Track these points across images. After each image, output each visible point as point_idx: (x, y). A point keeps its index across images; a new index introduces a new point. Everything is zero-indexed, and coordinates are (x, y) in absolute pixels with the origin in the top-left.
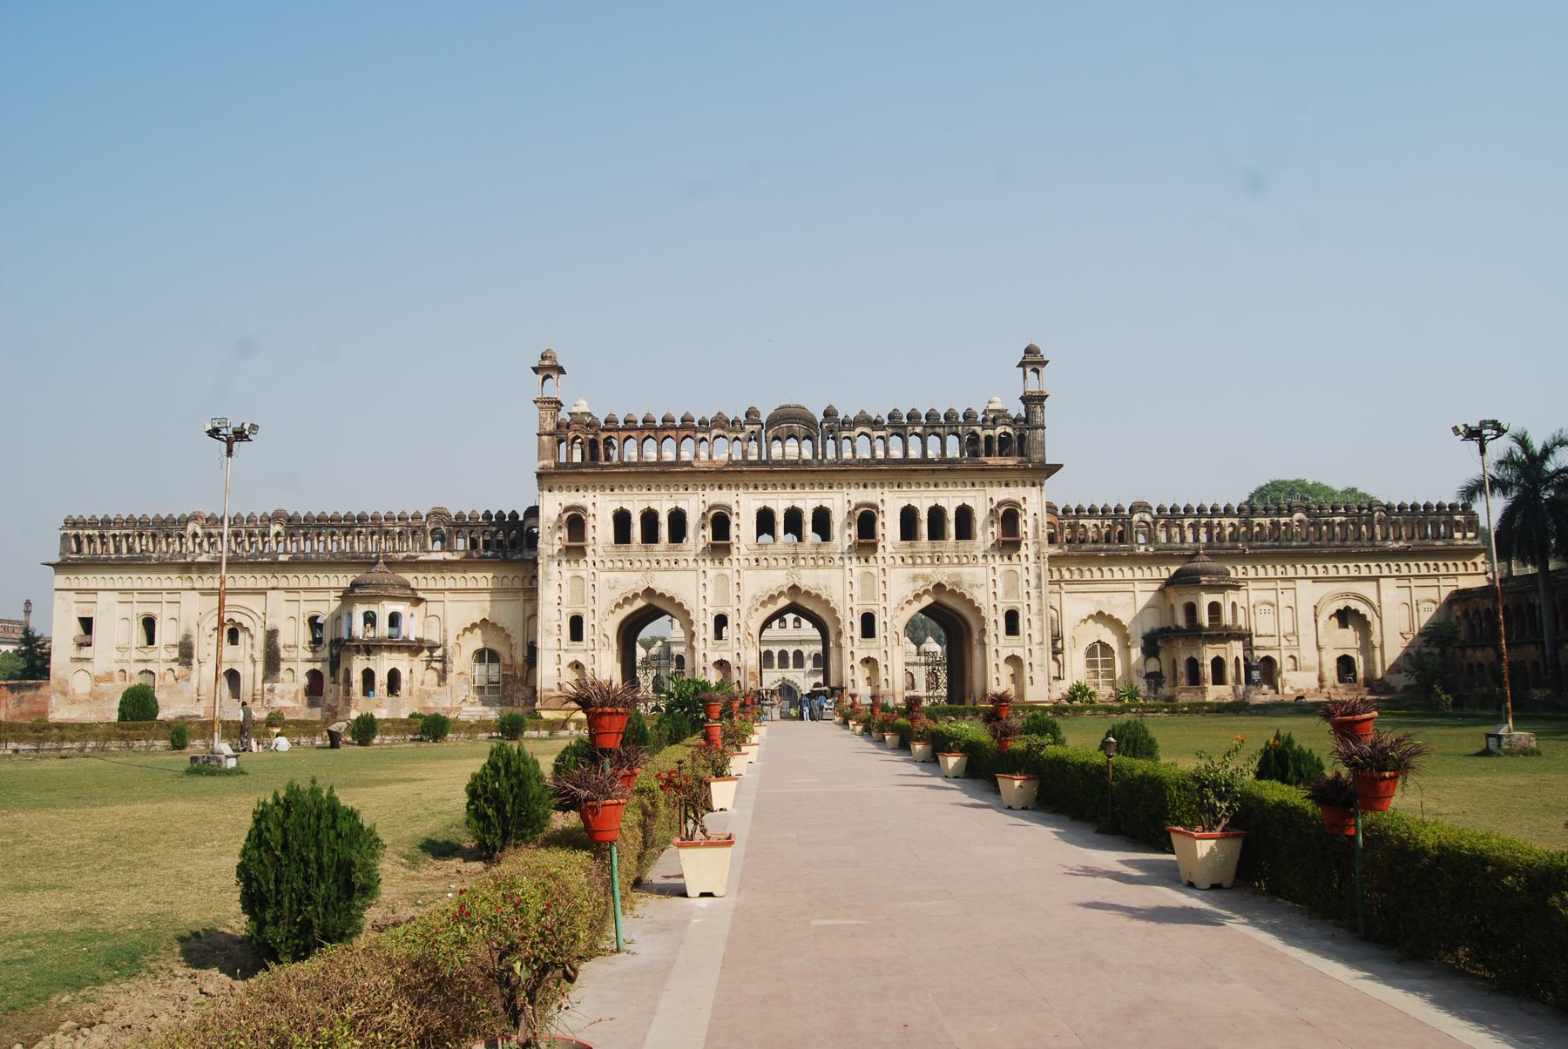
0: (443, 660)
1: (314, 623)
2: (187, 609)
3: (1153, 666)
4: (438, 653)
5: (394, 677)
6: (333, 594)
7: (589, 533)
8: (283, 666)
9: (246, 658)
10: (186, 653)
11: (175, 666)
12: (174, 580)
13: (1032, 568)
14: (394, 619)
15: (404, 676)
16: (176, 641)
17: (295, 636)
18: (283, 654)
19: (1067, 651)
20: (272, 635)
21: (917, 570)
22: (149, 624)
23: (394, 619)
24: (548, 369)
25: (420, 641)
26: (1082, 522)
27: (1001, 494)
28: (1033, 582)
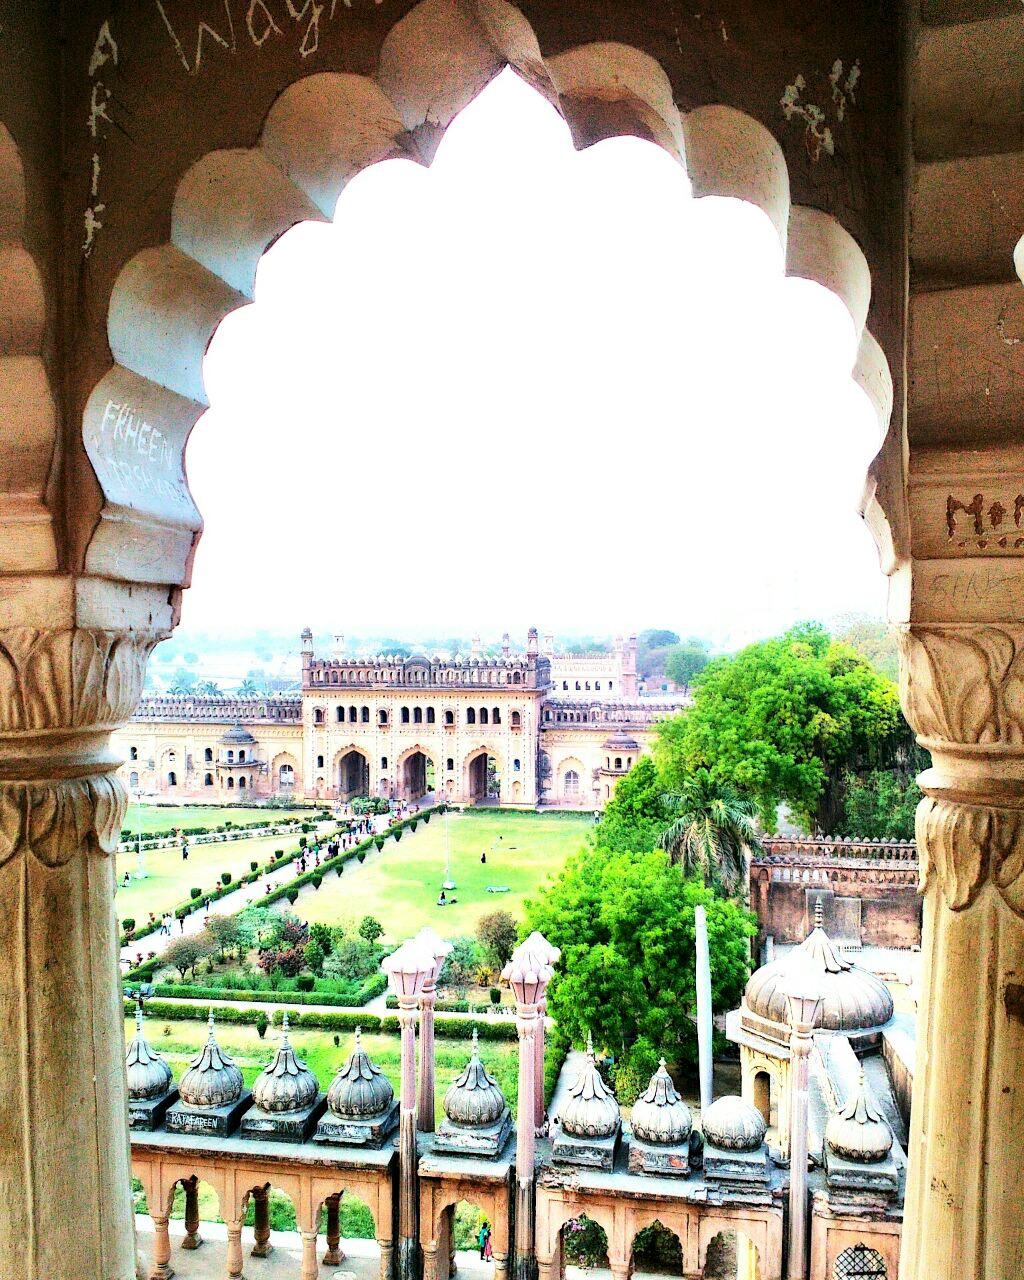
0: (267, 770)
1: (209, 752)
3: (597, 785)
4: (264, 767)
5: (242, 780)
6: (215, 739)
7: (326, 717)
8: (195, 771)
10: (152, 764)
13: (527, 741)
14: (242, 754)
15: (248, 779)
18: (195, 766)
19: (554, 778)
20: (189, 757)
21: (474, 739)
23: (242, 754)
24: (307, 636)
26: (565, 711)
27: (516, 704)
28: (527, 745)
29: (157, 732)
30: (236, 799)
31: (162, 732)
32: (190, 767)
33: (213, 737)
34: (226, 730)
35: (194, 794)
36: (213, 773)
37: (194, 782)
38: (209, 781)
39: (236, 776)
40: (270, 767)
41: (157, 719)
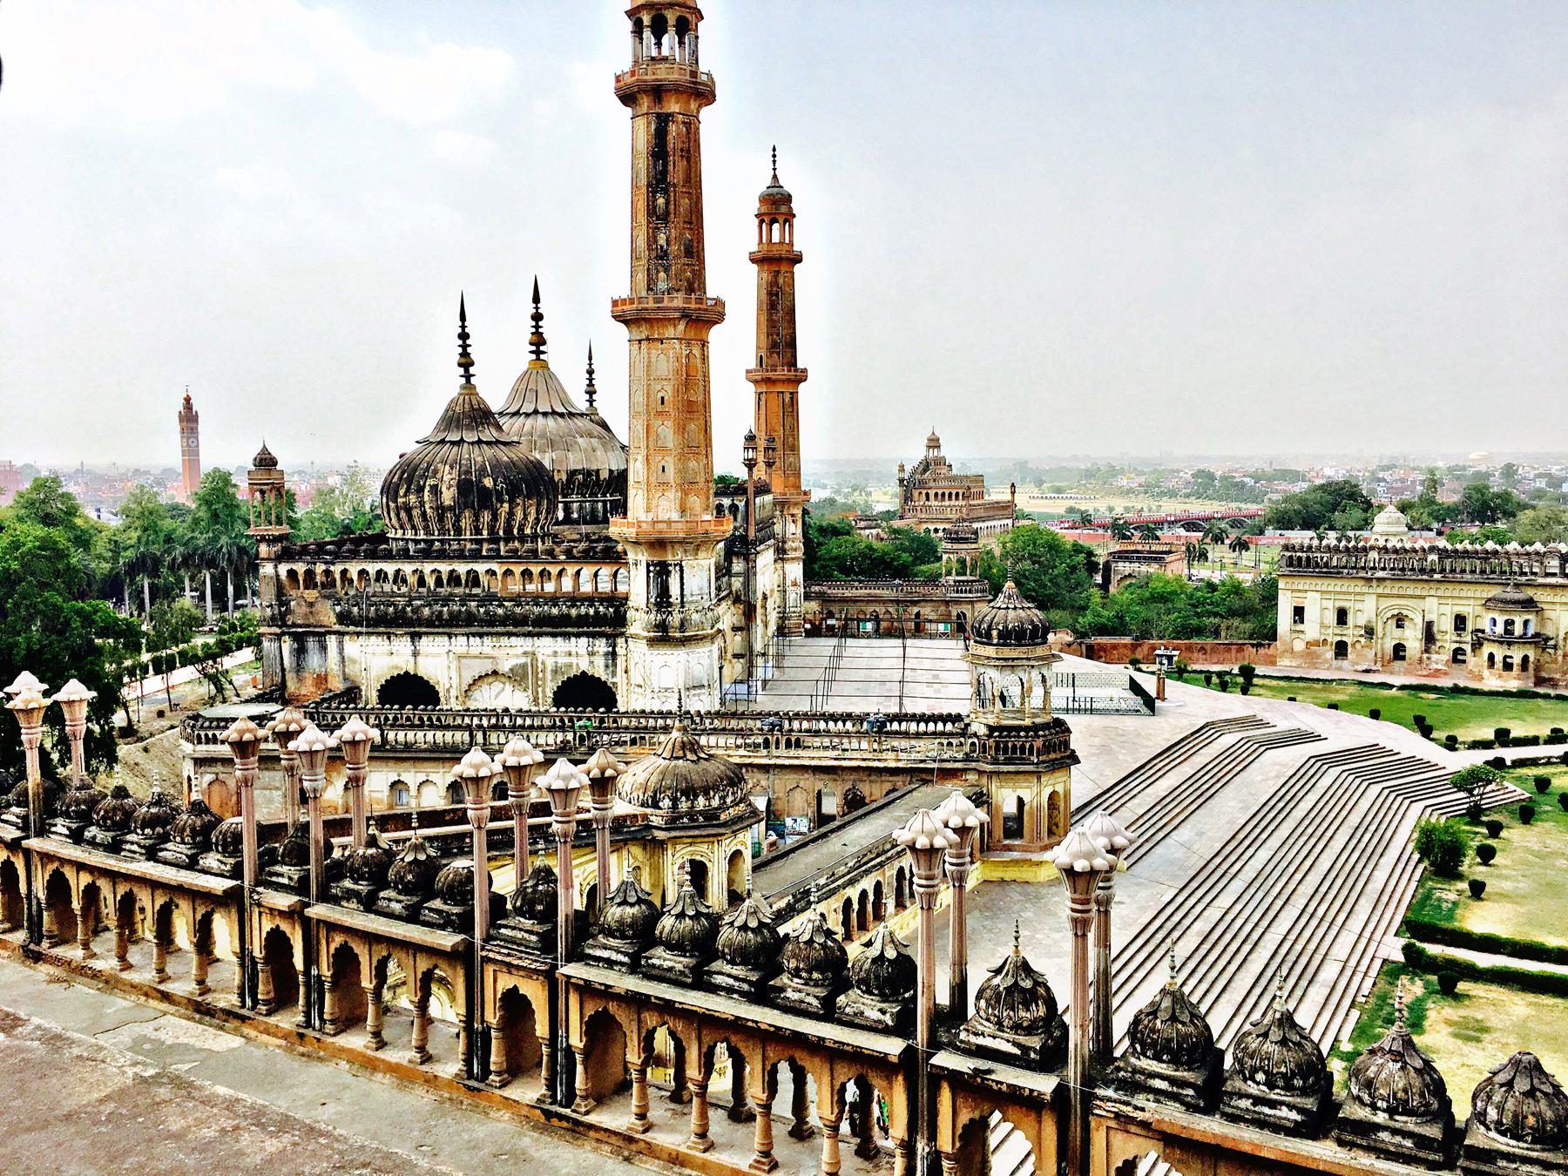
0: (1555, 647)
1: (1460, 622)
2: (1367, 606)
4: (1552, 643)
5: (1525, 659)
9: (1412, 638)
10: (1370, 632)
11: (1363, 640)
12: (1359, 587)
16: (1363, 623)
17: (1445, 625)
18: (1438, 636)
20: (1429, 626)
22: (1342, 616)
23: (1526, 623)
25: (1537, 635)
29: (1380, 590)
30: (1513, 683)
31: (1387, 591)
32: (1429, 637)
33: (1471, 601)
34: (1495, 592)
35: (1437, 673)
36: (1468, 648)
37: (1434, 657)
38: (1457, 657)
39: (1517, 655)
40: (1561, 643)
41: (1380, 574)
